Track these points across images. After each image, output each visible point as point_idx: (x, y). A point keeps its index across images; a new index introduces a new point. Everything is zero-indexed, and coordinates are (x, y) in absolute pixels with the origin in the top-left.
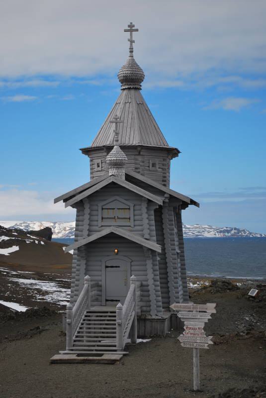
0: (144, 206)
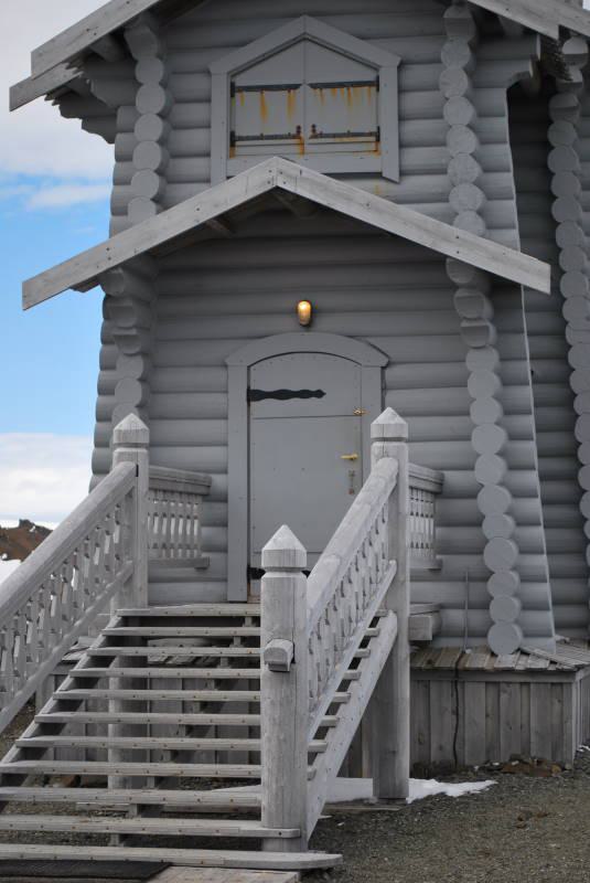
0: (456, 55)
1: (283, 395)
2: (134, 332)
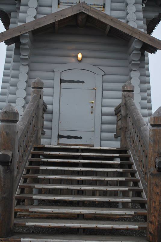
1: (71, 82)
2: (27, 57)
